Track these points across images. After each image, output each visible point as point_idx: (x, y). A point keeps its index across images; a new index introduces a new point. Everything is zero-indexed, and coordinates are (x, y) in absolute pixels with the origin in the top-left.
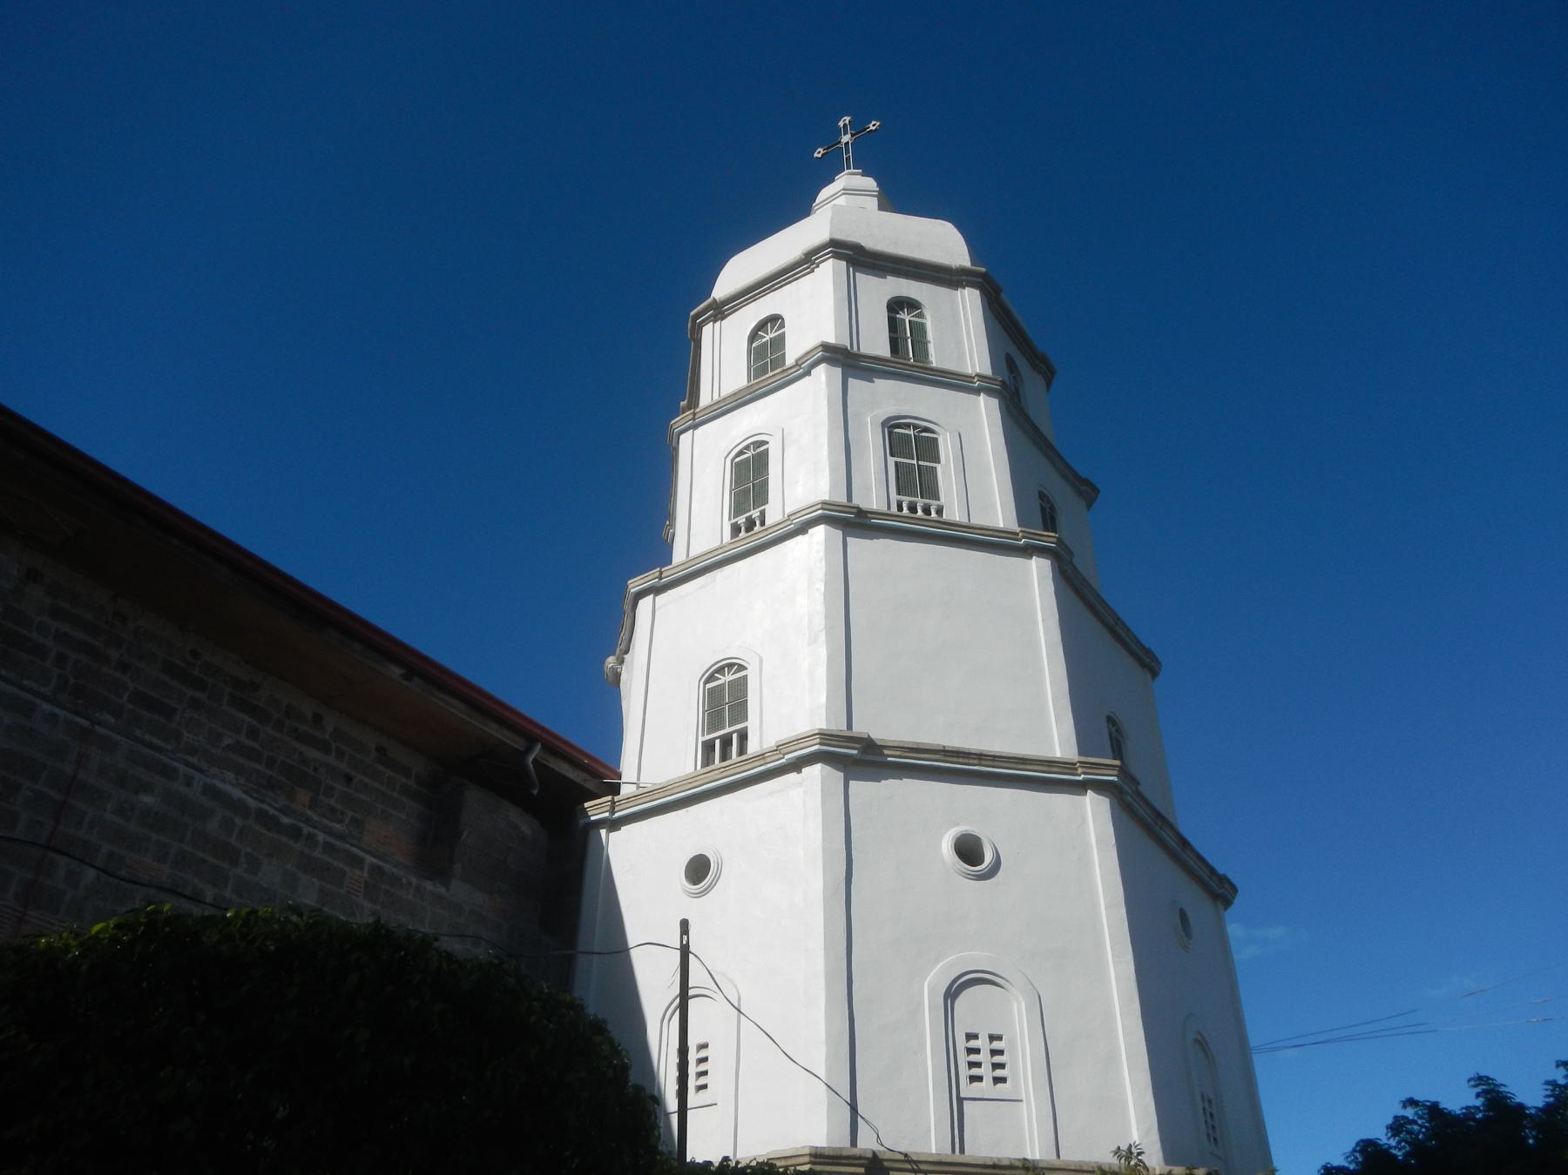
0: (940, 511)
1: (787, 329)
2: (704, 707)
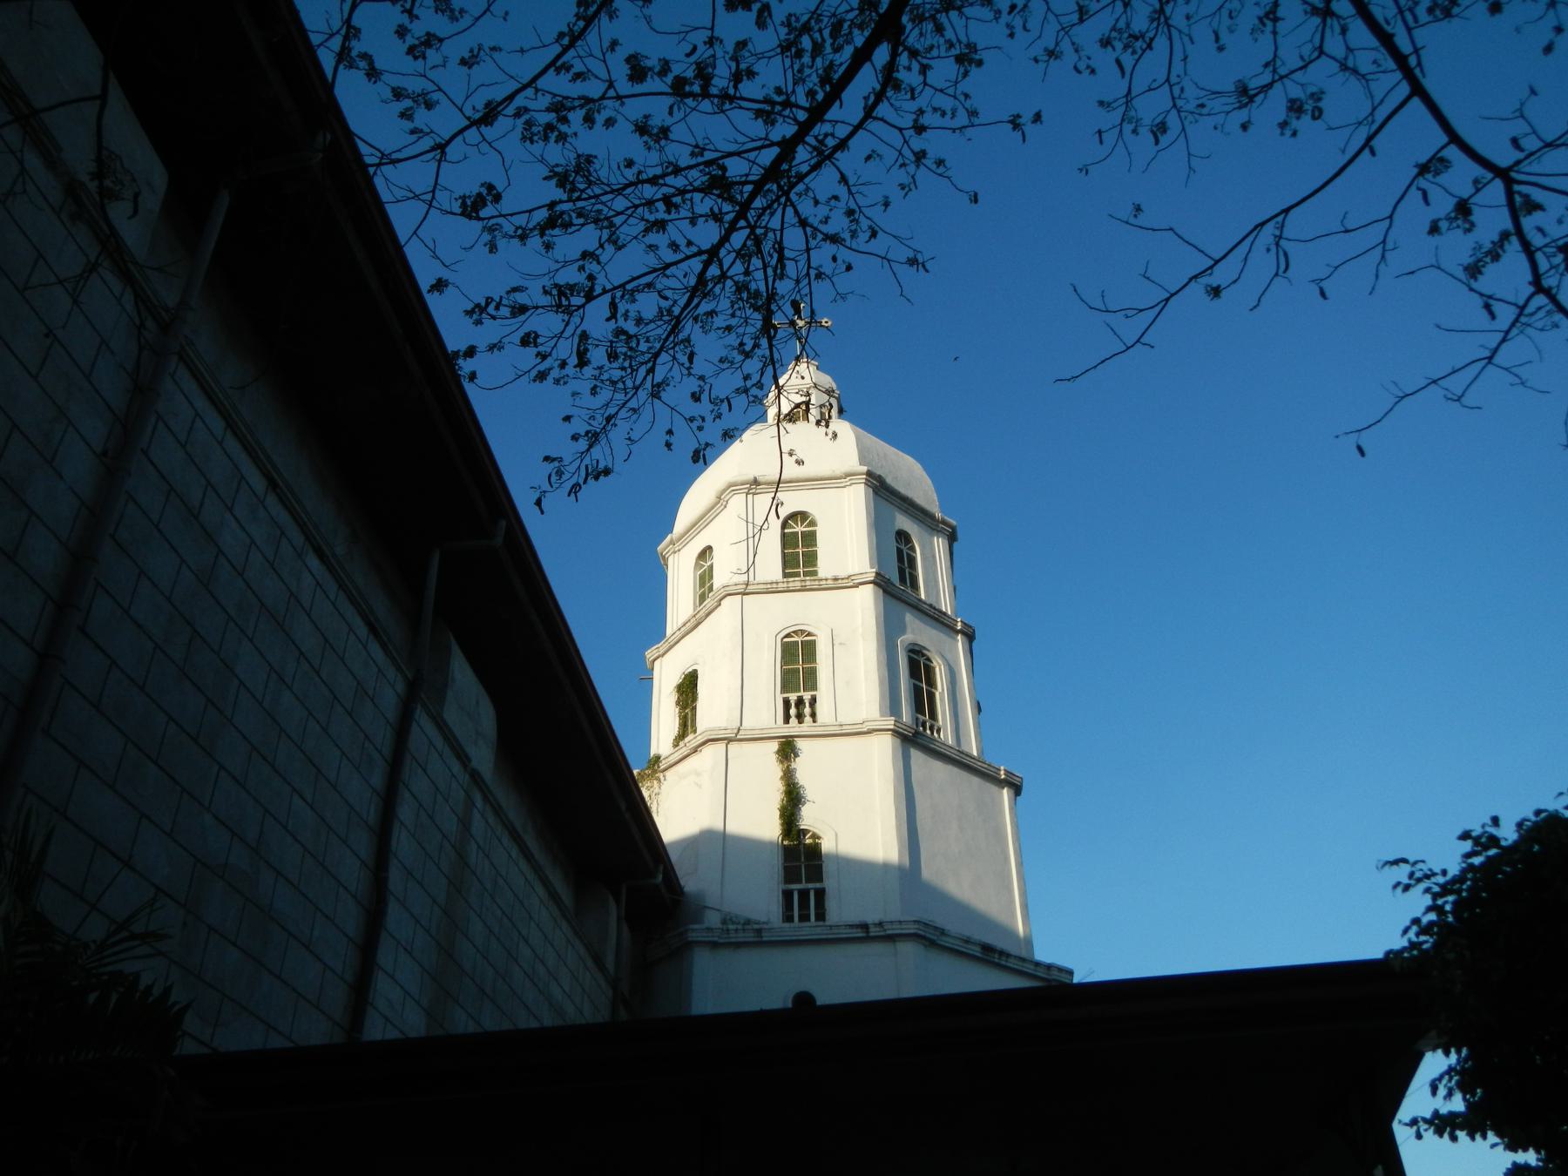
0: (939, 731)
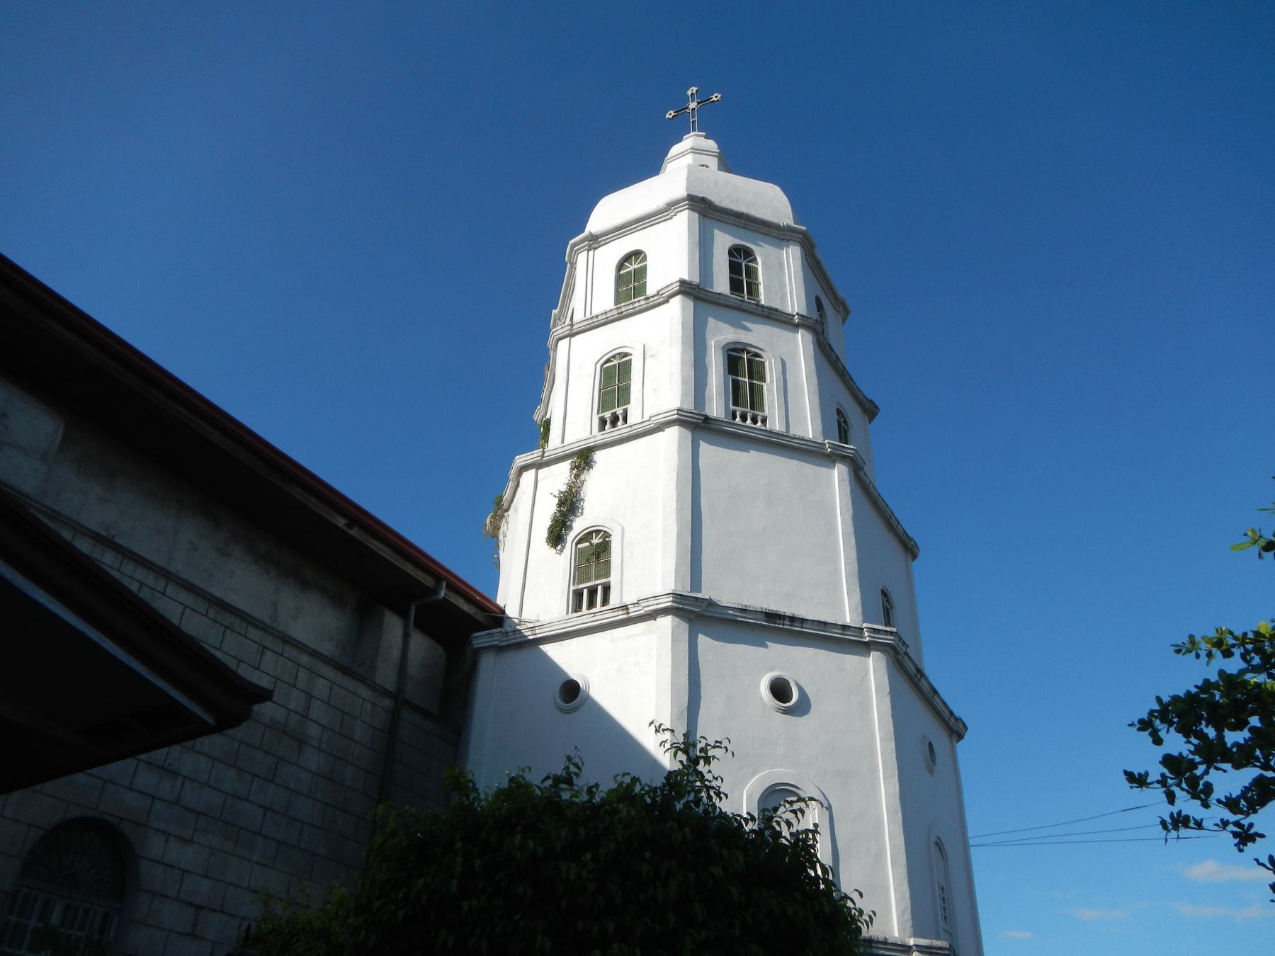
0: (764, 421)
1: (651, 264)
2: (575, 562)
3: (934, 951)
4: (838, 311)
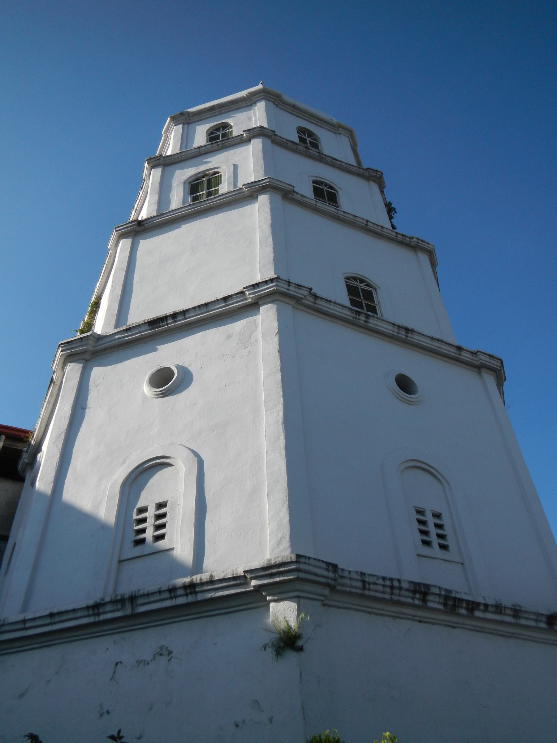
3: (274, 571)
4: (340, 134)
